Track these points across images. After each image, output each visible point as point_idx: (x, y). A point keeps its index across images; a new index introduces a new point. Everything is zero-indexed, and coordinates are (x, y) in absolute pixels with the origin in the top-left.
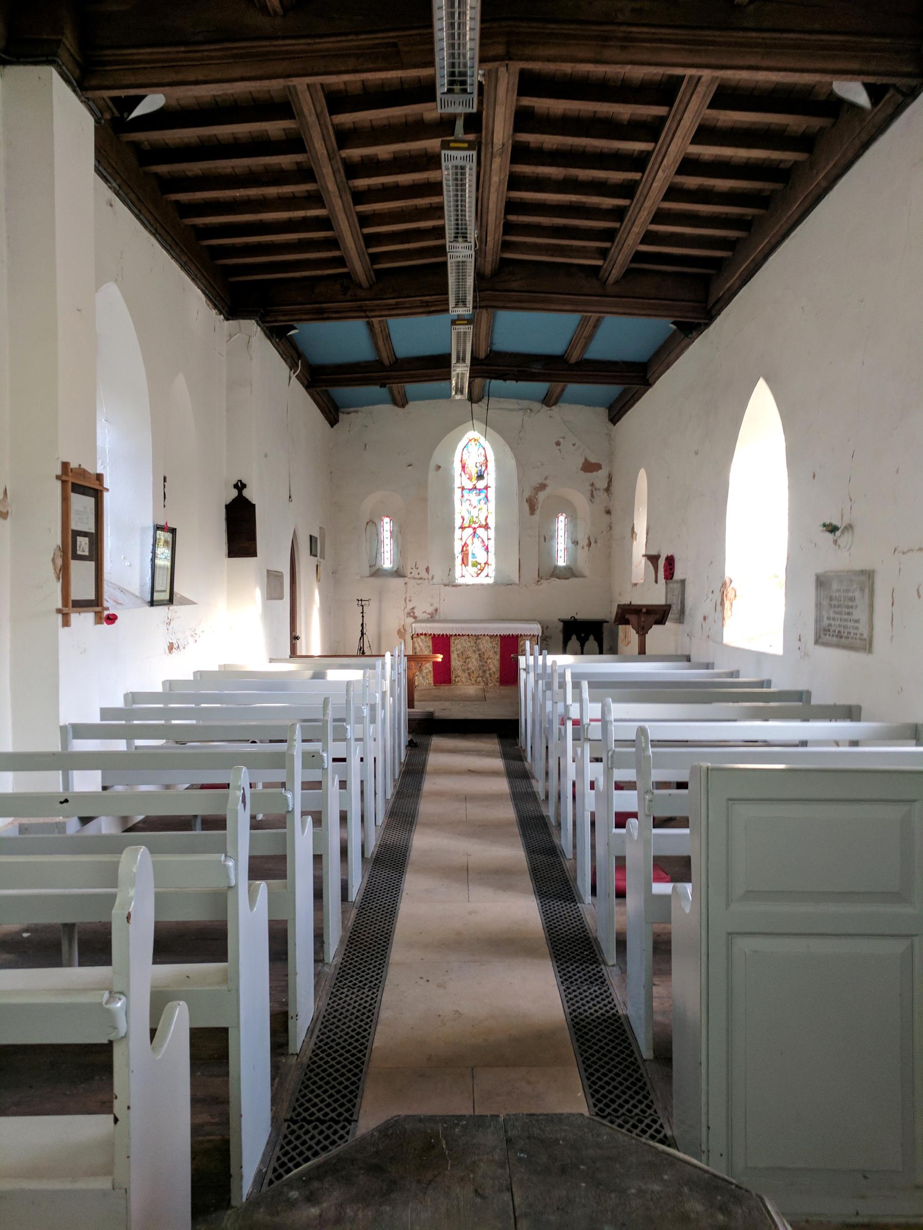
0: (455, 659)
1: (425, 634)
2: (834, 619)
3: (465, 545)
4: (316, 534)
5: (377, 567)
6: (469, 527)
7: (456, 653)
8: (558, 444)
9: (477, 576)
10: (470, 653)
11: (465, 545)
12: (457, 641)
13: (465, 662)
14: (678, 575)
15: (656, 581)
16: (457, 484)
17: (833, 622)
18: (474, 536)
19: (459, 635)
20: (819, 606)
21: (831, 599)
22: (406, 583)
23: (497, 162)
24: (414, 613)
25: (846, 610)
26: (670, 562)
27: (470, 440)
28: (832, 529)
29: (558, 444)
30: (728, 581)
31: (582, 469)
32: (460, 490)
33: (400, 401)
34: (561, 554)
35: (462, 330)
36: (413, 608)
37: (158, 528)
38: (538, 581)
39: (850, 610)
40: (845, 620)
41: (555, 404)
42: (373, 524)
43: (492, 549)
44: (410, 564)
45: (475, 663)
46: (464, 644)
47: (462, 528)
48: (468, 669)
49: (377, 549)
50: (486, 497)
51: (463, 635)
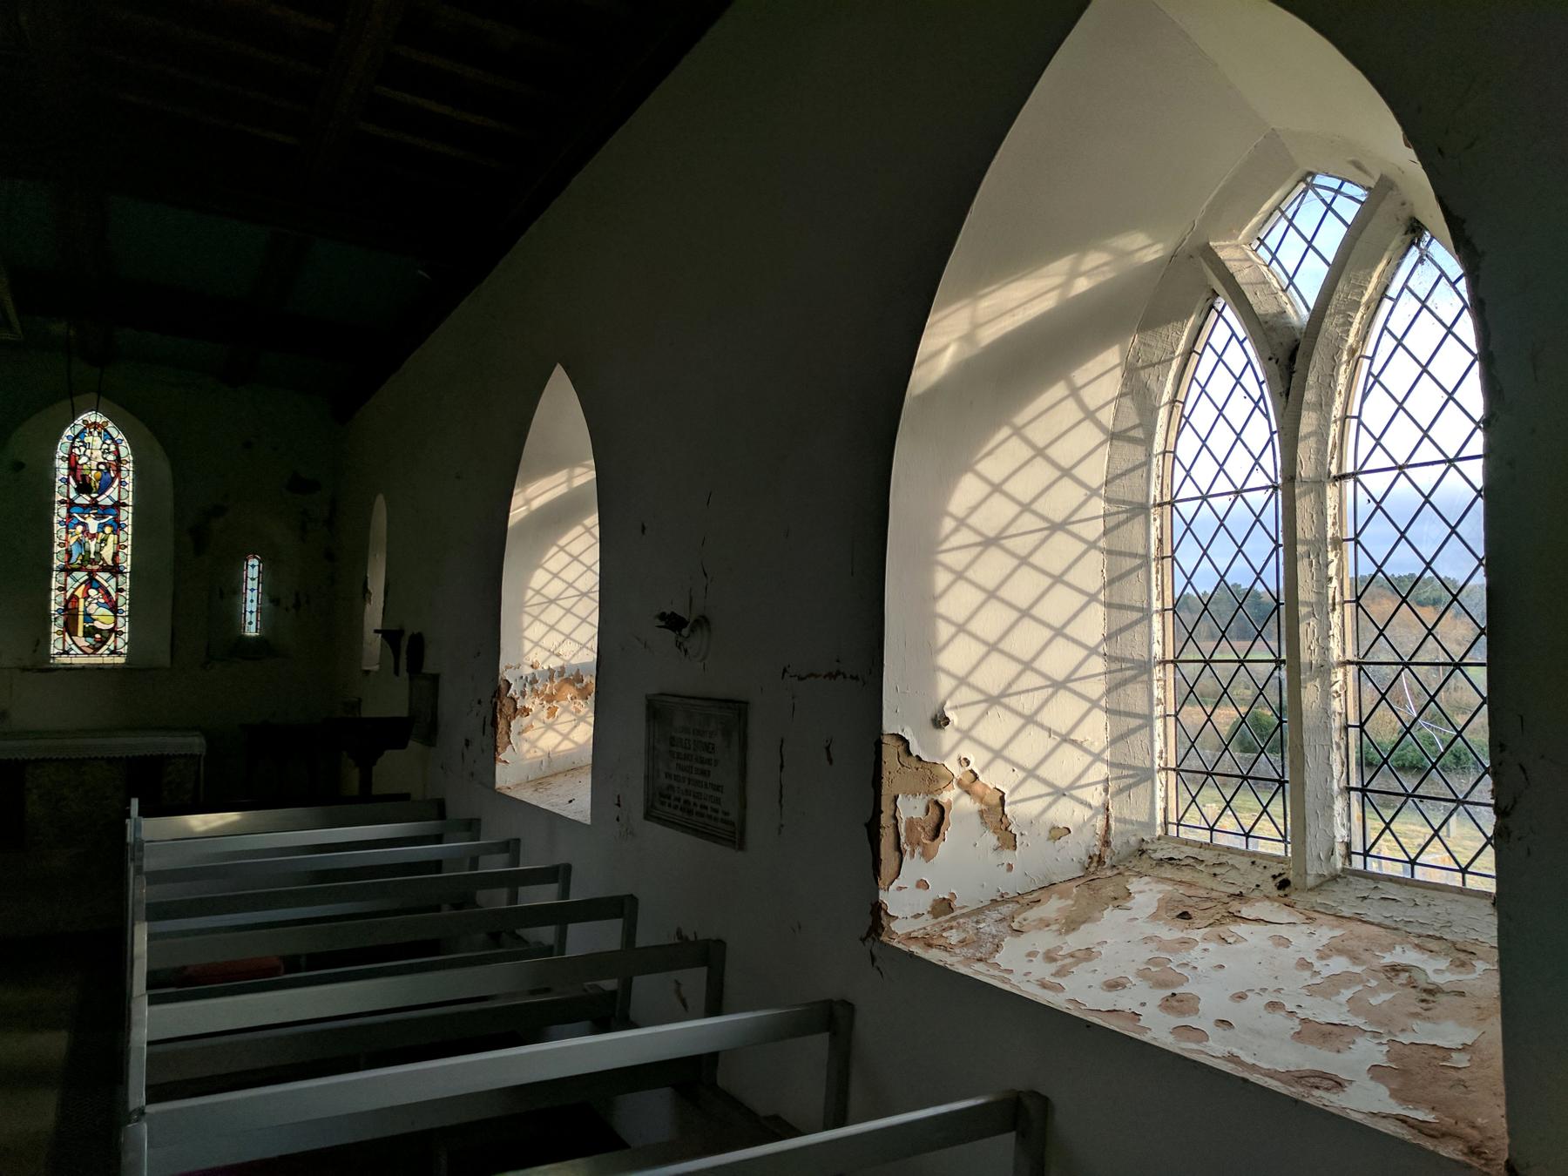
2: (677, 778)
15: (397, 672)
17: (675, 784)
20: (651, 752)
21: (672, 741)
25: (699, 766)
28: (673, 622)
39: (706, 767)
43: (125, 609)
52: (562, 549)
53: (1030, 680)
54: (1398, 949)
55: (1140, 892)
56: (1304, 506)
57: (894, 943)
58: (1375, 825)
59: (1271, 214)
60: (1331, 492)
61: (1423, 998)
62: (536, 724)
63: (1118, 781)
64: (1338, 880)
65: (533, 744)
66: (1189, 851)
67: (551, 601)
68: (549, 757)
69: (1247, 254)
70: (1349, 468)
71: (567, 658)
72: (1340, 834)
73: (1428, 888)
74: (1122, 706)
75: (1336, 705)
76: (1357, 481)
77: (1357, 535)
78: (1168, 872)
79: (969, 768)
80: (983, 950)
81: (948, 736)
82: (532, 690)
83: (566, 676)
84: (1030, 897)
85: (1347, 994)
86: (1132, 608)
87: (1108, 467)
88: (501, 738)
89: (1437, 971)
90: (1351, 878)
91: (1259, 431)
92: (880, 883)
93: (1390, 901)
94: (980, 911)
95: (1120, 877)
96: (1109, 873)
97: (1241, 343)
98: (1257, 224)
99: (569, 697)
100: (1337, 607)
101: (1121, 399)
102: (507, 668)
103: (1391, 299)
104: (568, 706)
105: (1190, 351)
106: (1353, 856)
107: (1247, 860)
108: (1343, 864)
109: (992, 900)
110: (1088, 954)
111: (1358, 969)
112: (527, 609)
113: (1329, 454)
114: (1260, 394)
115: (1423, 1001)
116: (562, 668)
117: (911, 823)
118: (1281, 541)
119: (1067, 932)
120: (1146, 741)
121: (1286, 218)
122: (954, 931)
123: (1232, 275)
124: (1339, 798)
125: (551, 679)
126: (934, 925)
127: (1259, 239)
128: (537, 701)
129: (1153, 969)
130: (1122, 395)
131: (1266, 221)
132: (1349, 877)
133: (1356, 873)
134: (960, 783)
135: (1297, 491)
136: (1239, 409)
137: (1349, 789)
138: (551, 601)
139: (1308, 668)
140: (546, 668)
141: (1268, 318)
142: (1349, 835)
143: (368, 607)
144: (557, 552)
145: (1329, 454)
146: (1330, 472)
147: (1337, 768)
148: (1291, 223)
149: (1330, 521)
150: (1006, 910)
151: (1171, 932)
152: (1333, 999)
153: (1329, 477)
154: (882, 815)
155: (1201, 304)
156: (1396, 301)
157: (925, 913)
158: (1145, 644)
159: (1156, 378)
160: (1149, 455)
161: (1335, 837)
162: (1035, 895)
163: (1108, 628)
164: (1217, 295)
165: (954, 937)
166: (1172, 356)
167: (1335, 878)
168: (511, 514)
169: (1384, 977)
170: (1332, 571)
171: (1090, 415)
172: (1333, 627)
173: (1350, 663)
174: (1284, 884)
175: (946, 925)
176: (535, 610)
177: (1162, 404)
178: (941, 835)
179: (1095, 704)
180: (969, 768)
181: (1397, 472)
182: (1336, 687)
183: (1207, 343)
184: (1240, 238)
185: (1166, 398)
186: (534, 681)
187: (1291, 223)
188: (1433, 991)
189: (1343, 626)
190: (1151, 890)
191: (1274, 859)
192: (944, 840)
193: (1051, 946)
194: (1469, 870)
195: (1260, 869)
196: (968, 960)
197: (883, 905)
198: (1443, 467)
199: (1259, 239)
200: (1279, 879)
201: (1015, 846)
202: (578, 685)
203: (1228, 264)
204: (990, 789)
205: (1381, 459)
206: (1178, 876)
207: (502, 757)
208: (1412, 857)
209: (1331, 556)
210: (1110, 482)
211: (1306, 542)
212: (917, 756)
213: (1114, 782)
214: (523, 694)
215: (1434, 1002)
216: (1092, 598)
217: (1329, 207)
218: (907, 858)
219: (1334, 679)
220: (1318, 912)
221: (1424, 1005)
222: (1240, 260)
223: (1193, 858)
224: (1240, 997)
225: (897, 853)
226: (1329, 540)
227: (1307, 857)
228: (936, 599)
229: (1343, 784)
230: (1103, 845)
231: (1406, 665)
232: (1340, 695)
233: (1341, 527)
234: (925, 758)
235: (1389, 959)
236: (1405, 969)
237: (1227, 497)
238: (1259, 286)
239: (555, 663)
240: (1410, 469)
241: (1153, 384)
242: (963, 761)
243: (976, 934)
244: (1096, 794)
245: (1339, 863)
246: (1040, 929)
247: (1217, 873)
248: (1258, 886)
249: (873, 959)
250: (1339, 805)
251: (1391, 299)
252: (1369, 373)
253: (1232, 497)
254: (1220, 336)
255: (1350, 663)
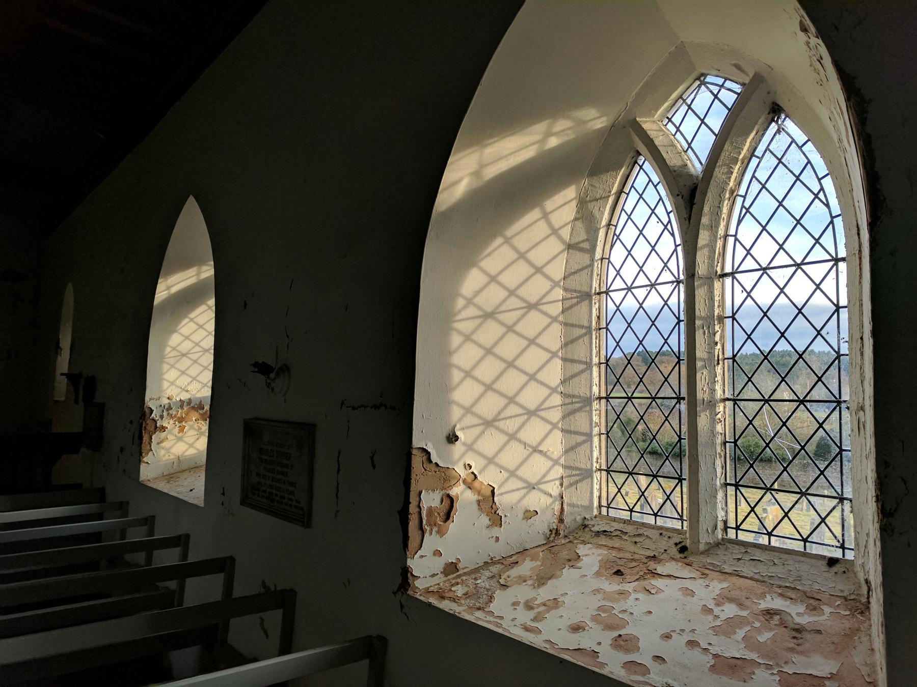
17: (263, 481)
20: (246, 458)
26: (91, 383)
39: (285, 470)
52: (192, 320)
53: (513, 410)
54: (768, 597)
55: (586, 555)
56: (701, 294)
57: (418, 596)
58: (744, 508)
59: (676, 101)
60: (717, 285)
61: (794, 636)
62: (170, 437)
63: (570, 478)
64: (720, 546)
65: (168, 451)
66: (616, 526)
67: (183, 355)
68: (179, 459)
69: (661, 128)
70: (728, 269)
71: (193, 393)
72: (721, 515)
73: (781, 552)
74: (572, 427)
75: (719, 428)
76: (734, 278)
77: (734, 314)
78: (603, 540)
79: (471, 470)
80: (481, 600)
81: (458, 448)
82: (168, 414)
83: (192, 405)
84: (511, 559)
85: (741, 633)
86: (580, 362)
87: (566, 267)
88: (145, 447)
89: (798, 614)
90: (729, 545)
91: (667, 245)
92: (408, 553)
93: (757, 561)
94: (477, 570)
95: (571, 544)
96: (563, 541)
97: (655, 186)
98: (668, 106)
99: (194, 419)
100: (720, 362)
101: (575, 222)
102: (151, 399)
103: (758, 157)
104: (193, 425)
105: (620, 192)
106: (728, 529)
107: (657, 532)
108: (723, 535)
109: (485, 562)
110: (555, 604)
111: (744, 613)
112: (165, 360)
113: (716, 259)
114: (668, 220)
115: (794, 638)
116: (190, 399)
117: (430, 510)
118: (682, 318)
119: (539, 586)
120: (588, 451)
121: (686, 104)
122: (459, 586)
123: (652, 140)
124: (720, 490)
125: (182, 407)
126: (445, 582)
127: (667, 118)
128: (172, 422)
129: (603, 615)
130: (576, 219)
131: (674, 105)
132: (727, 544)
133: (731, 541)
134: (464, 481)
135: (696, 284)
136: (653, 230)
137: (726, 485)
138: (183, 355)
139: (702, 403)
140: (178, 399)
141: (676, 169)
142: (726, 516)
143: (59, 358)
144: (189, 322)
145: (716, 259)
146: (717, 272)
147: (719, 470)
148: (689, 107)
149: (716, 304)
150: (495, 569)
151: (611, 586)
152: (732, 637)
153: (716, 275)
154: (410, 505)
155: (628, 160)
156: (761, 159)
157: (439, 573)
158: (588, 386)
159: (598, 208)
160: (592, 260)
161: (717, 517)
162: (514, 558)
163: (564, 375)
164: (639, 154)
165: (460, 590)
166: (609, 194)
167: (717, 545)
168: (156, 296)
169: (764, 619)
170: (717, 338)
171: (555, 232)
172: (717, 376)
173: (728, 399)
174: (683, 549)
175: (453, 582)
176: (172, 361)
177: (602, 226)
178: (451, 518)
179: (554, 426)
180: (471, 470)
181: (762, 272)
182: (719, 416)
183: (632, 186)
184: (656, 116)
185: (604, 222)
186: (170, 408)
187: (689, 107)
188: (799, 630)
189: (724, 375)
190: (593, 554)
191: (675, 532)
192: (453, 522)
193: (529, 597)
194: (809, 540)
195: (666, 539)
196: (471, 609)
197: (410, 569)
198: (794, 268)
199: (667, 118)
200: (680, 546)
201: (501, 524)
202: (201, 412)
203: (649, 132)
204: (485, 485)
205: (749, 264)
206: (610, 543)
207: (145, 459)
208: (770, 531)
209: (717, 328)
210: (566, 277)
211: (701, 318)
212: (436, 463)
213: (566, 479)
214: (162, 417)
215: (801, 638)
216: (554, 354)
217: (716, 97)
218: (427, 535)
219: (718, 411)
220: (709, 569)
221: (795, 641)
222: (656, 131)
223: (620, 531)
224: (667, 637)
225: (420, 532)
226: (715, 317)
227: (700, 531)
228: (450, 353)
229: (723, 481)
230: (559, 522)
231: (767, 401)
232: (721, 421)
233: (723, 309)
234: (441, 464)
235: (765, 604)
236: (776, 612)
237: (645, 288)
238: (670, 148)
239: (185, 396)
240: (771, 270)
241: (596, 213)
242: (467, 466)
243: (475, 588)
244: (555, 488)
245: (719, 534)
246: (520, 584)
247: (637, 541)
248: (665, 550)
249: (402, 607)
250: (720, 495)
251: (758, 157)
252: (743, 206)
253: (649, 288)
254: (642, 180)
255: (728, 399)
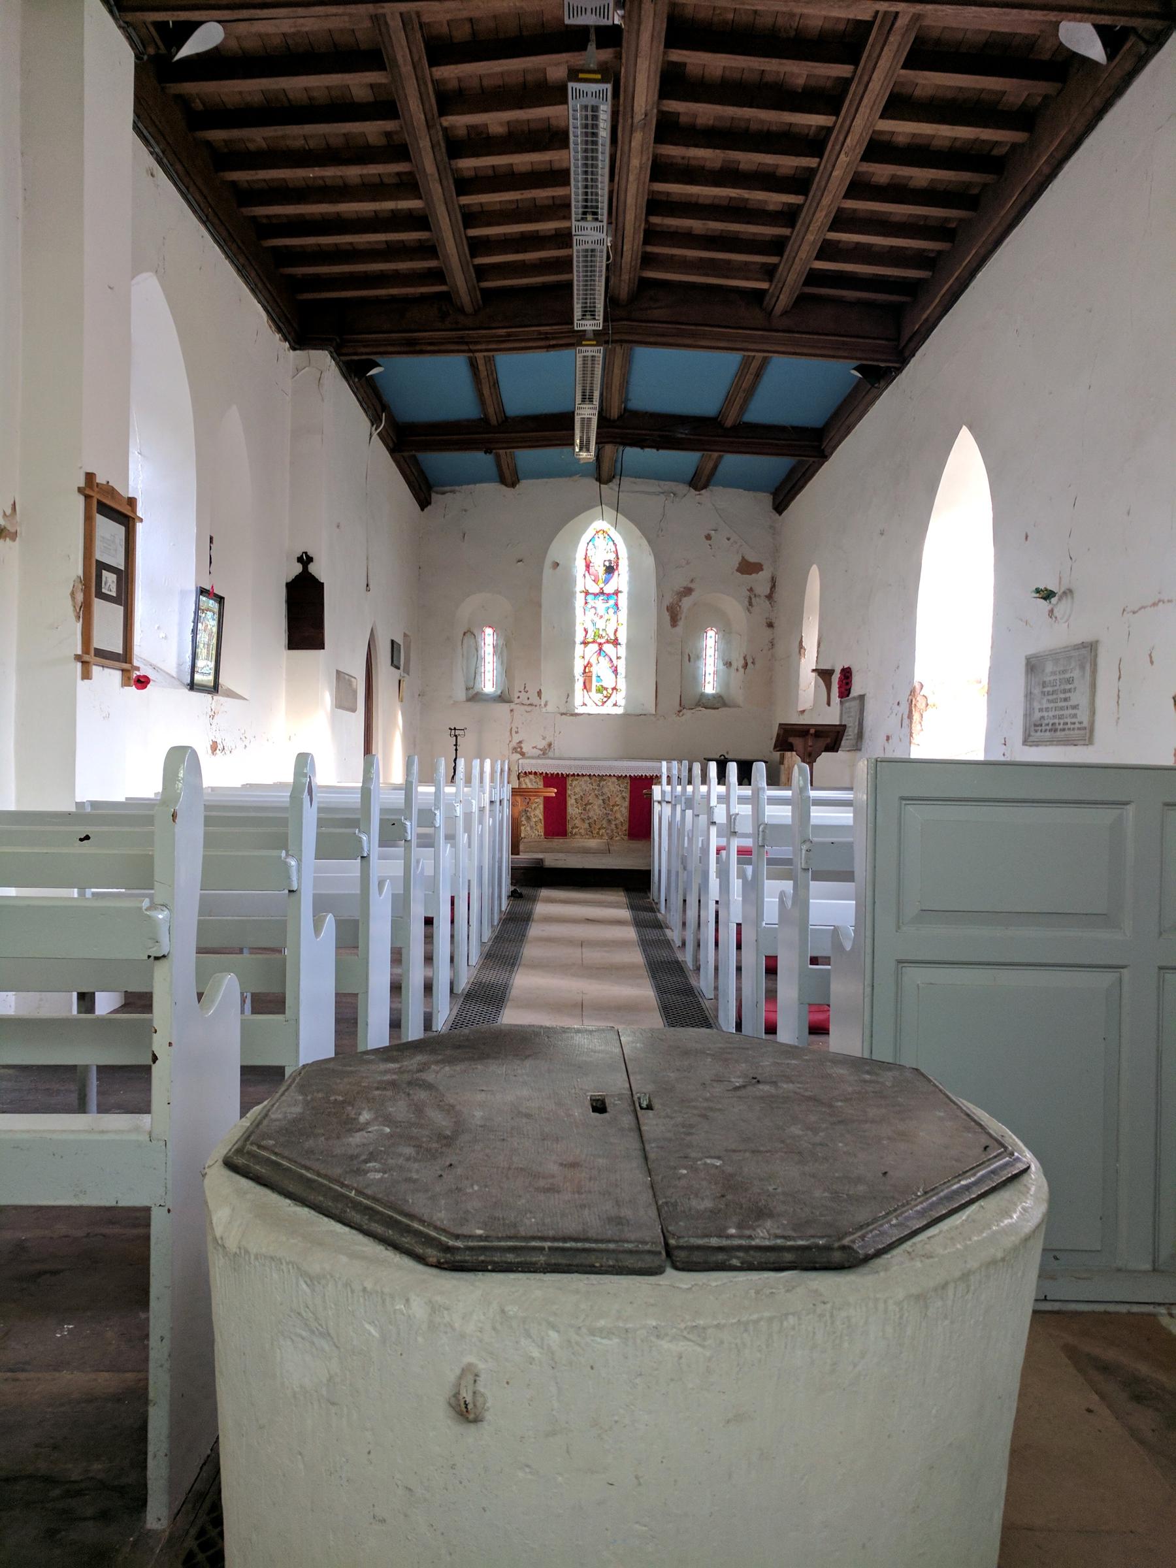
0: (572, 805)
1: (535, 773)
2: (1047, 709)
3: (589, 664)
4: (399, 640)
5: (476, 690)
6: (594, 642)
7: (573, 797)
8: (708, 537)
9: (603, 705)
10: (591, 798)
11: (589, 664)
12: (575, 783)
13: (585, 809)
14: (856, 691)
16: (579, 587)
17: (1045, 714)
18: (599, 654)
19: (578, 775)
20: (1029, 696)
21: (1044, 684)
22: (512, 711)
23: (638, 137)
24: (521, 748)
25: (1063, 696)
27: (597, 532)
29: (708, 537)
30: (918, 687)
31: (737, 570)
32: (583, 594)
33: (509, 478)
34: (709, 678)
35: (590, 354)
36: (520, 742)
37: (203, 592)
38: (679, 711)
39: (1067, 695)
40: (1062, 708)
41: (705, 487)
42: (471, 633)
43: (622, 670)
44: (518, 685)
45: (598, 812)
46: (584, 787)
47: (585, 643)
48: (589, 818)
49: (476, 668)
50: (616, 605)
51: (583, 775)
